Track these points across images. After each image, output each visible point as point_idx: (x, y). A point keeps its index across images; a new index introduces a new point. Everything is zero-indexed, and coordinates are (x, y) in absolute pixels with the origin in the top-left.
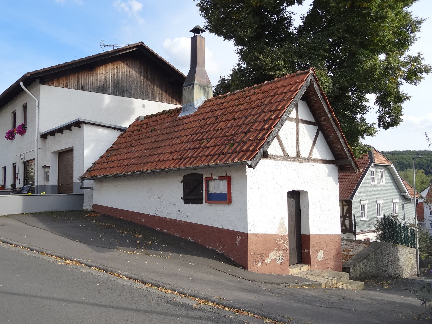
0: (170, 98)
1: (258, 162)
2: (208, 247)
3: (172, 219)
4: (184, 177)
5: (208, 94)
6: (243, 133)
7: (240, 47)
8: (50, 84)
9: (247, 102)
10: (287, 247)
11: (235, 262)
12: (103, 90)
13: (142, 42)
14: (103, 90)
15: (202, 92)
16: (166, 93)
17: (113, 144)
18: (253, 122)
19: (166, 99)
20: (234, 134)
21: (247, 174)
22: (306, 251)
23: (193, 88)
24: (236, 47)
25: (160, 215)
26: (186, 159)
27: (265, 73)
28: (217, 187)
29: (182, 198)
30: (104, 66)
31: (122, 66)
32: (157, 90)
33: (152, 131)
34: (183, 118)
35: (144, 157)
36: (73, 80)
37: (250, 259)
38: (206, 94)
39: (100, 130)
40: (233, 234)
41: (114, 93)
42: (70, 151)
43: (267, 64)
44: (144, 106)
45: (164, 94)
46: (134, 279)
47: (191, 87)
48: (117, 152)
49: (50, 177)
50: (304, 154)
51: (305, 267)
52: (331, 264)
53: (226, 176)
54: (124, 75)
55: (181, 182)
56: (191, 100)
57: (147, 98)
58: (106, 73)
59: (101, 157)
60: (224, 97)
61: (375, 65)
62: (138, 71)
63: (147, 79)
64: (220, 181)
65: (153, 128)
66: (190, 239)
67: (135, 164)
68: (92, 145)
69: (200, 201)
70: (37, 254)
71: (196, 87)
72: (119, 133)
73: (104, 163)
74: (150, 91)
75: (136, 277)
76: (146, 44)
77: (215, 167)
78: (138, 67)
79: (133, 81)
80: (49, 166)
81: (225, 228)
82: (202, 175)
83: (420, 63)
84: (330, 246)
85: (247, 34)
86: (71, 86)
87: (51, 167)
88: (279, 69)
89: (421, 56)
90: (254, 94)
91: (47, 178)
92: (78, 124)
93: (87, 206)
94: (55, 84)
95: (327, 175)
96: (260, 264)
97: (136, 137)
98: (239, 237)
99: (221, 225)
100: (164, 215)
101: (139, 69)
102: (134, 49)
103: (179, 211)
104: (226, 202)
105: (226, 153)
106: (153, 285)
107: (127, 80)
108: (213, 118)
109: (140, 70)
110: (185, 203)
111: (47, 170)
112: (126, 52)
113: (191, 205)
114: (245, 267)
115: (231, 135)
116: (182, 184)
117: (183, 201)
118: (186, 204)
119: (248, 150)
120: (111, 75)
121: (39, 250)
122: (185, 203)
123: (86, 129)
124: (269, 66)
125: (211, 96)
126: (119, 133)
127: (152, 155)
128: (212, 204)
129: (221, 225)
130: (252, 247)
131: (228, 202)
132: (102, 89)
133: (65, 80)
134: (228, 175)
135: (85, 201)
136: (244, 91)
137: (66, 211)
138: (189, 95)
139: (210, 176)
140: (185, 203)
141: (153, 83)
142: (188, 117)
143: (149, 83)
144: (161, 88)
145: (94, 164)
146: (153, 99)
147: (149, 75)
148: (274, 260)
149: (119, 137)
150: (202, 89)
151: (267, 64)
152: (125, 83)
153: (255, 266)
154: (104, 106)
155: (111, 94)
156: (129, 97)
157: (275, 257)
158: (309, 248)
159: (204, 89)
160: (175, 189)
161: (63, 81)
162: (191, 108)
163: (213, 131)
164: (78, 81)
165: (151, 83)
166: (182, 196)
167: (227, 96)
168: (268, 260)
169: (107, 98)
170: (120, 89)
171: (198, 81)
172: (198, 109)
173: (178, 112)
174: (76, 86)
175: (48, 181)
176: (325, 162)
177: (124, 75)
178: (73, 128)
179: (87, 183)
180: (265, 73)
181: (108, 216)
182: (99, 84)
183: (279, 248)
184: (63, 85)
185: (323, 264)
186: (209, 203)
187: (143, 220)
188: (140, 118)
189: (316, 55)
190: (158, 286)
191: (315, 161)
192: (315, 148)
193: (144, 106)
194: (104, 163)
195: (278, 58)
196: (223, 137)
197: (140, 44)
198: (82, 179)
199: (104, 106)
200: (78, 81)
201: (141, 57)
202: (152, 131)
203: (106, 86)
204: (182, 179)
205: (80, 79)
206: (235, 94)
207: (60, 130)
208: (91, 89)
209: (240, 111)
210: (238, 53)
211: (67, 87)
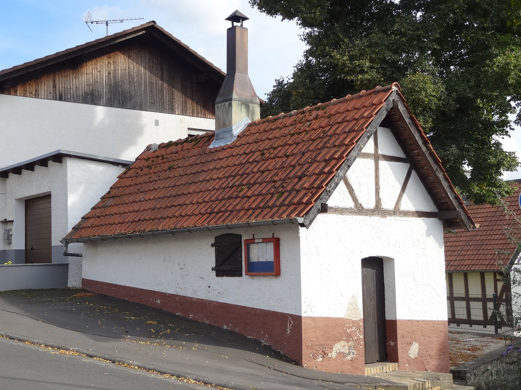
0: (199, 108)
1: (314, 219)
4: (216, 238)
5: (253, 113)
6: (297, 177)
7: (308, 30)
8: (12, 92)
9: (305, 131)
10: (362, 337)
11: (286, 357)
12: (93, 99)
13: (154, 22)
14: (93, 99)
15: (244, 111)
16: (192, 100)
17: (111, 188)
18: (311, 162)
19: (193, 110)
20: (284, 179)
21: (300, 235)
22: (392, 344)
23: (230, 105)
24: (303, 29)
25: (183, 294)
26: (218, 213)
27: (340, 78)
28: (261, 253)
29: (213, 269)
30: (94, 61)
31: (123, 60)
32: (178, 96)
33: (170, 168)
34: (216, 151)
35: (159, 209)
36: (46, 85)
37: (305, 351)
38: (250, 113)
39: (93, 166)
41: (110, 104)
42: (47, 197)
44: (157, 123)
45: (189, 101)
46: (149, 370)
47: (227, 103)
48: (117, 201)
49: (13, 238)
50: (388, 204)
51: (390, 367)
52: (433, 363)
53: (273, 238)
54: (124, 74)
55: (212, 246)
56: (228, 124)
57: (162, 110)
58: (97, 72)
59: (94, 208)
60: (275, 120)
61: (509, 64)
62: (147, 67)
63: (162, 79)
64: (264, 244)
65: (171, 164)
66: (225, 327)
67: (145, 219)
69: (236, 272)
70: (20, 343)
71: (234, 104)
72: (120, 170)
73: (99, 217)
75: (152, 367)
77: (255, 226)
78: (147, 61)
79: (140, 83)
80: (12, 221)
81: (272, 309)
82: (240, 236)
84: (429, 337)
85: (315, 15)
86: (43, 95)
87: (14, 222)
88: (362, 72)
90: (316, 118)
91: (8, 239)
92: (59, 158)
93: (73, 282)
94: (18, 92)
95: (424, 233)
96: (321, 359)
97: (146, 179)
98: (290, 322)
100: (188, 293)
101: (149, 63)
102: (141, 33)
103: (209, 287)
105: (272, 205)
106: (172, 375)
107: (130, 82)
108: (258, 153)
109: (151, 65)
111: (9, 227)
112: (128, 38)
114: (298, 362)
116: (214, 249)
117: (214, 273)
118: (219, 278)
119: (300, 203)
120: (105, 74)
121: (22, 338)
123: (71, 165)
124: (347, 67)
125: (257, 117)
126: (120, 170)
127: (170, 207)
128: (254, 277)
130: (308, 336)
131: (275, 273)
132: (91, 98)
134: (275, 236)
135: (70, 274)
136: (303, 112)
137: (43, 290)
138: (225, 115)
139: (251, 237)
140: (218, 275)
141: (171, 85)
142: (223, 149)
143: (165, 85)
144: (184, 92)
145: (83, 218)
146: (172, 111)
147: (165, 73)
148: (342, 355)
149: (120, 177)
150: (243, 107)
151: (344, 64)
152: (126, 87)
153: (312, 362)
155: (106, 105)
156: (134, 108)
157: (342, 350)
158: (395, 339)
159: (247, 107)
160: (203, 256)
161: (31, 88)
162: (227, 136)
163: (257, 172)
164: (55, 87)
165: (169, 85)
166: (214, 265)
167: (279, 118)
168: (333, 354)
169: (100, 112)
170: (120, 97)
171: (237, 95)
172: (238, 136)
173: (208, 140)
174: (52, 95)
175: (10, 244)
176: (421, 214)
177: (124, 74)
178: (50, 163)
179: (73, 247)
180: (340, 78)
181: (105, 296)
182: (87, 89)
183: (348, 337)
184: (32, 93)
185: (419, 363)
186: (251, 276)
187: (159, 302)
188: (152, 147)
190: (178, 377)
191: (406, 214)
192: (405, 195)
193: (157, 123)
194: (99, 217)
195: (361, 55)
196: (270, 182)
197: (150, 25)
198: (66, 241)
200: (55, 87)
201: (152, 44)
202: (170, 168)
203: (97, 93)
204: (213, 241)
205: (57, 82)
206: (291, 116)
208: (73, 98)
209: (295, 143)
210: (305, 39)
211: (37, 96)
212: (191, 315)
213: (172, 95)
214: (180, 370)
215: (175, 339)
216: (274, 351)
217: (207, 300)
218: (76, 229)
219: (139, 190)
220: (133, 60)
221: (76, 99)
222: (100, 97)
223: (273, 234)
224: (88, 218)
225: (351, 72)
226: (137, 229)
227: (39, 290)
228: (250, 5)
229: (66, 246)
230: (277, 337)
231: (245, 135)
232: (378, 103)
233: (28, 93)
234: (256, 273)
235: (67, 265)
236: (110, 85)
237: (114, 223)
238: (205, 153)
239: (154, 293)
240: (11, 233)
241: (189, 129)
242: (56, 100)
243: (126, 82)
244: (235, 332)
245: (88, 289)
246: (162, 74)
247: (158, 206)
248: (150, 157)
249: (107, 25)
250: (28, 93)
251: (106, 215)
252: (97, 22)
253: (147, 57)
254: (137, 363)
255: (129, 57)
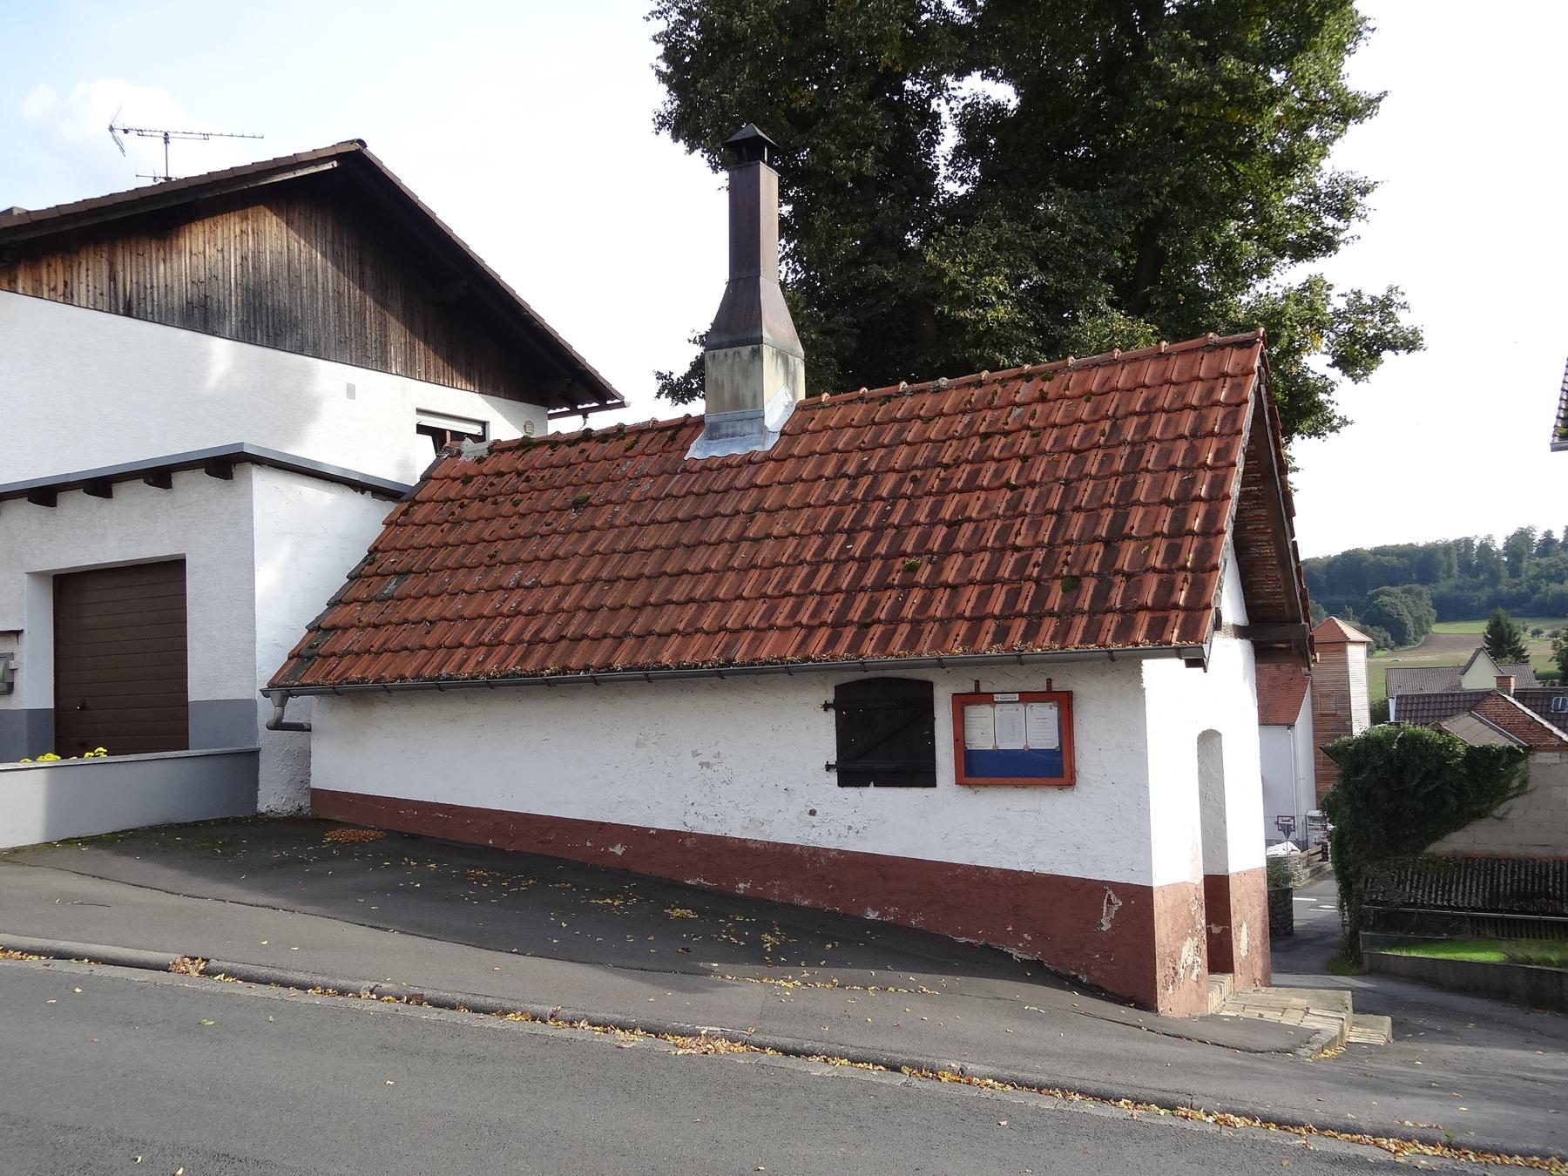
2: (963, 940)
3: (775, 844)
4: (839, 689)
5: (794, 379)
6: (1095, 540)
12: (206, 321)
13: (361, 142)
14: (206, 321)
15: (781, 371)
16: (426, 342)
17: (373, 551)
19: (427, 366)
20: (1051, 544)
21: (1145, 684)
23: (757, 354)
25: (710, 829)
26: (868, 626)
27: (941, 313)
29: (828, 767)
30: (208, 222)
31: (275, 229)
32: (397, 334)
33: (576, 505)
34: (706, 468)
35: (613, 609)
36: (90, 274)
39: (311, 492)
40: (1086, 893)
41: (246, 335)
42: (173, 568)
43: (953, 282)
44: (351, 391)
47: (746, 351)
48: (410, 585)
49: (20, 681)
55: (826, 707)
56: (749, 400)
58: (214, 251)
60: (888, 398)
62: (329, 252)
63: (362, 287)
64: (1021, 706)
65: (584, 492)
66: (872, 915)
68: (284, 551)
70: (492, 1022)
71: (767, 352)
74: (372, 333)
75: (1044, 1079)
76: (376, 150)
79: (314, 290)
80: (18, 633)
81: (1046, 870)
82: (928, 687)
83: (1387, 317)
85: (860, 165)
87: (25, 637)
89: (1397, 299)
92: (224, 465)
93: (274, 796)
94: (20, 284)
99: (1026, 862)
100: (735, 829)
101: (333, 242)
102: (328, 166)
104: (1057, 780)
107: (291, 286)
109: (337, 247)
110: (842, 783)
112: (300, 173)
113: (872, 792)
114: (1146, 1002)
115: (1039, 545)
116: (832, 713)
117: (833, 777)
119: (1164, 605)
120: (234, 260)
121: (480, 1001)
122: (842, 783)
123: (264, 487)
124: (959, 288)
126: (386, 509)
128: (982, 789)
129: (1026, 862)
132: (200, 315)
133: (60, 269)
134: (1056, 687)
135: (262, 776)
136: (980, 384)
137: (206, 823)
138: (738, 378)
139: (970, 688)
140: (842, 783)
141: (382, 303)
142: (748, 461)
143: (369, 302)
144: (409, 322)
145: (314, 628)
146: (383, 366)
149: (389, 523)
151: (954, 285)
152: (283, 297)
154: (211, 383)
156: (301, 352)
159: (786, 363)
160: (807, 733)
161: (54, 275)
163: (933, 524)
164: (113, 278)
166: (833, 760)
169: (222, 356)
170: (266, 320)
171: (770, 331)
172: (783, 433)
173: (672, 439)
174: (106, 298)
177: (279, 264)
178: (179, 479)
179: (297, 710)
180: (941, 313)
182: (194, 293)
184: (55, 289)
186: (969, 785)
187: (618, 850)
189: (1086, 262)
190: (1171, 1107)
193: (351, 391)
194: (376, 626)
196: (1003, 549)
197: (353, 148)
198: (282, 688)
199: (211, 383)
200: (113, 278)
201: (350, 200)
202: (576, 505)
203: (215, 305)
204: (830, 697)
205: (120, 268)
207: (101, 486)
208: (160, 313)
211: (68, 298)
212: (741, 886)
213: (383, 327)
214: (1171, 1084)
215: (793, 962)
216: (1056, 974)
217: (802, 847)
218: (301, 657)
219: (492, 557)
220: (298, 232)
221: (163, 317)
222: (221, 315)
223: (1049, 681)
224: (334, 628)
225: (965, 301)
226: (574, 662)
227: (196, 824)
228: (653, 127)
229: (282, 704)
230: (1086, 941)
231: (805, 431)
232: (1238, 371)
233: (45, 288)
234: (980, 780)
235: (254, 754)
236: (247, 289)
237: (461, 645)
238: (684, 470)
239: (601, 826)
240: (13, 665)
241: (420, 411)
242: (117, 313)
243: (283, 283)
244: (909, 929)
245: (338, 818)
246: (362, 273)
247: (609, 601)
248: (471, 472)
249: (166, 141)
250: (45, 288)
251: (406, 621)
252: (140, 133)
253: (329, 228)
254: (988, 1069)
255: (289, 223)
